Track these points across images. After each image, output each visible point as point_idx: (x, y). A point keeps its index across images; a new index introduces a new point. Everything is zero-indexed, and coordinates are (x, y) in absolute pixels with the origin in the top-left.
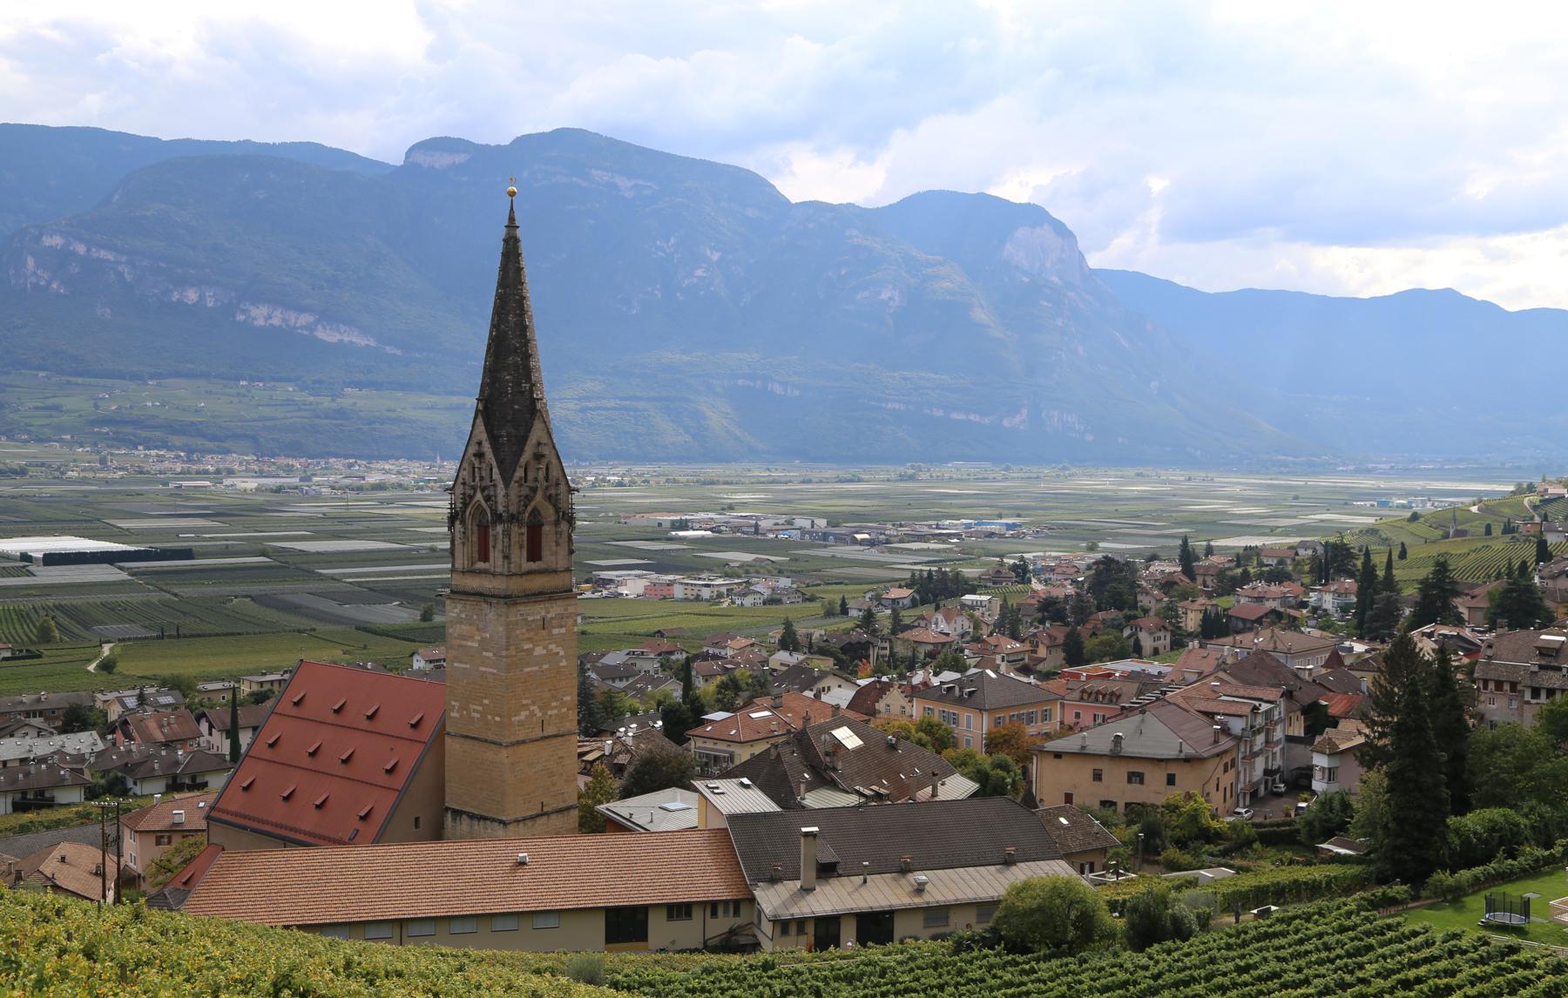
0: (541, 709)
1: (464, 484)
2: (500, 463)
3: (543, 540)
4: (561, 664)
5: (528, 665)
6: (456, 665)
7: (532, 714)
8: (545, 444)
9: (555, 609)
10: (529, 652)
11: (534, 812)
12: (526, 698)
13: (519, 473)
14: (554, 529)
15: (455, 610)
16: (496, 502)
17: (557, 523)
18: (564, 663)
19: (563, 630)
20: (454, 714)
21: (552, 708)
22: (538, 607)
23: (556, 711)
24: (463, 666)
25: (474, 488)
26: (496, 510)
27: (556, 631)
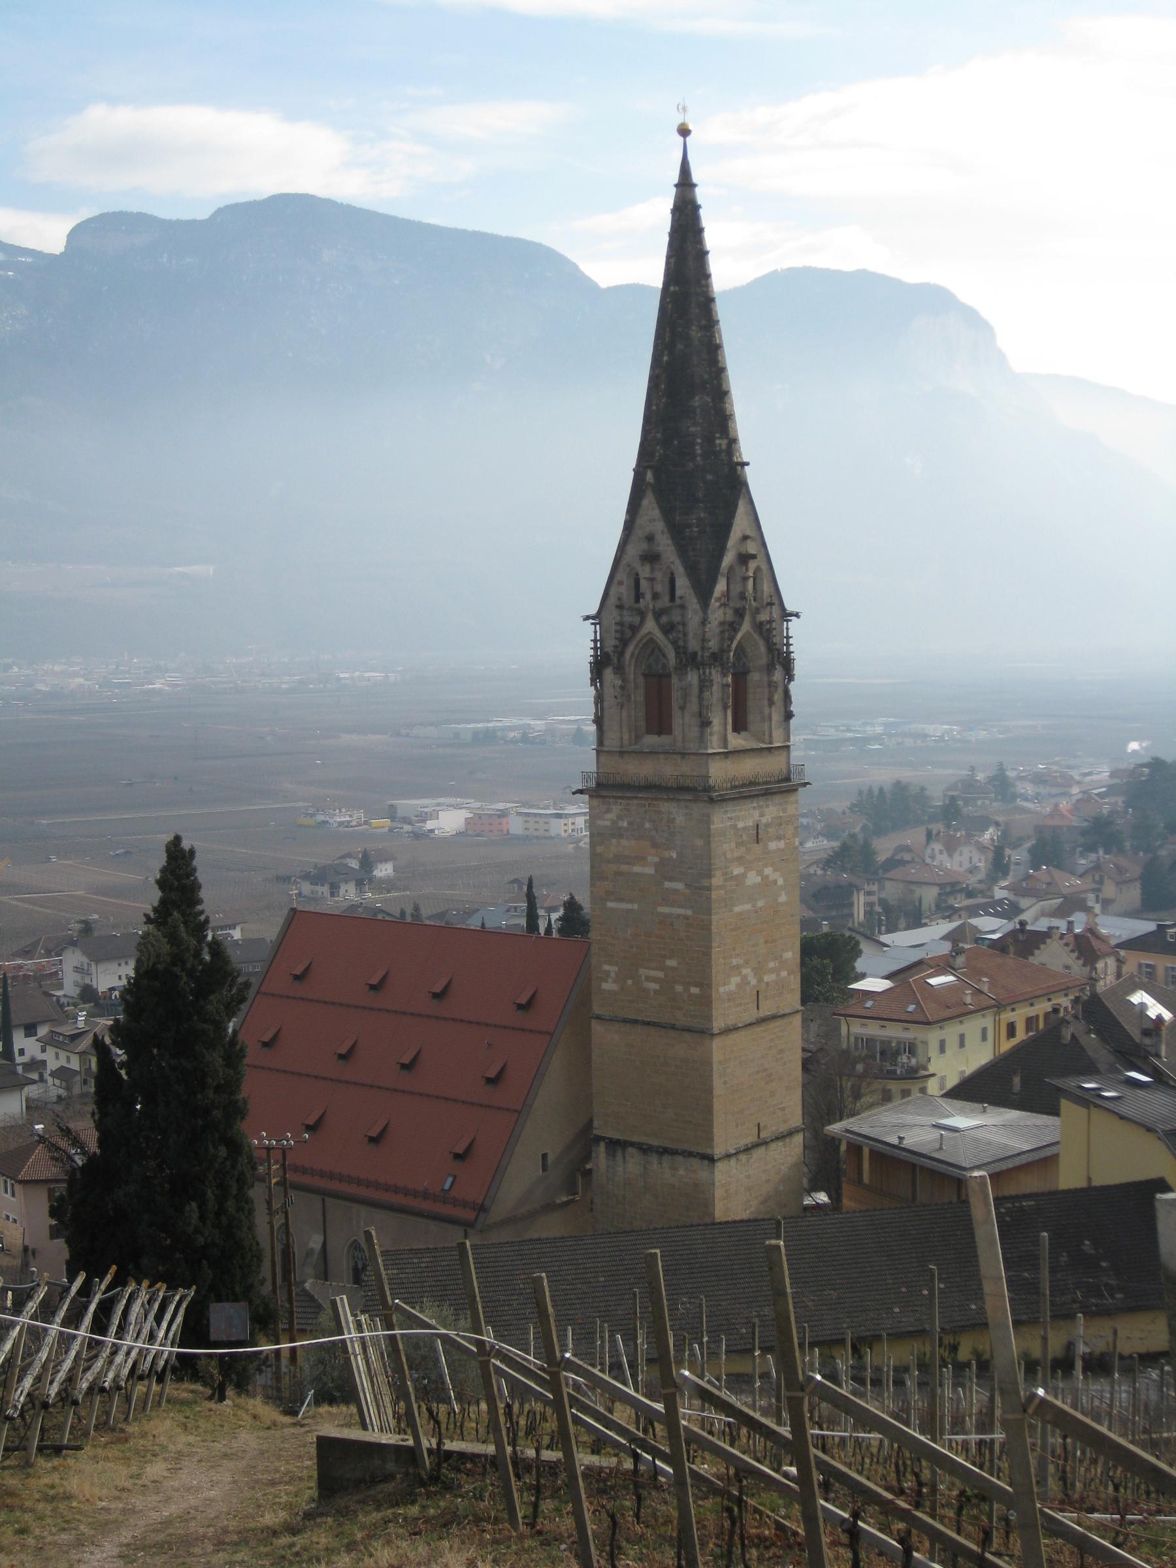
1: (620, 607)
2: (691, 570)
3: (750, 697)
6: (610, 905)
7: (745, 981)
9: (768, 812)
10: (739, 879)
11: (743, 1142)
12: (737, 955)
13: (721, 587)
14: (765, 678)
15: (609, 816)
16: (685, 635)
17: (770, 668)
18: (783, 898)
19: (782, 844)
20: (609, 986)
23: (773, 977)
24: (629, 906)
25: (642, 614)
26: (685, 647)
27: (773, 845)
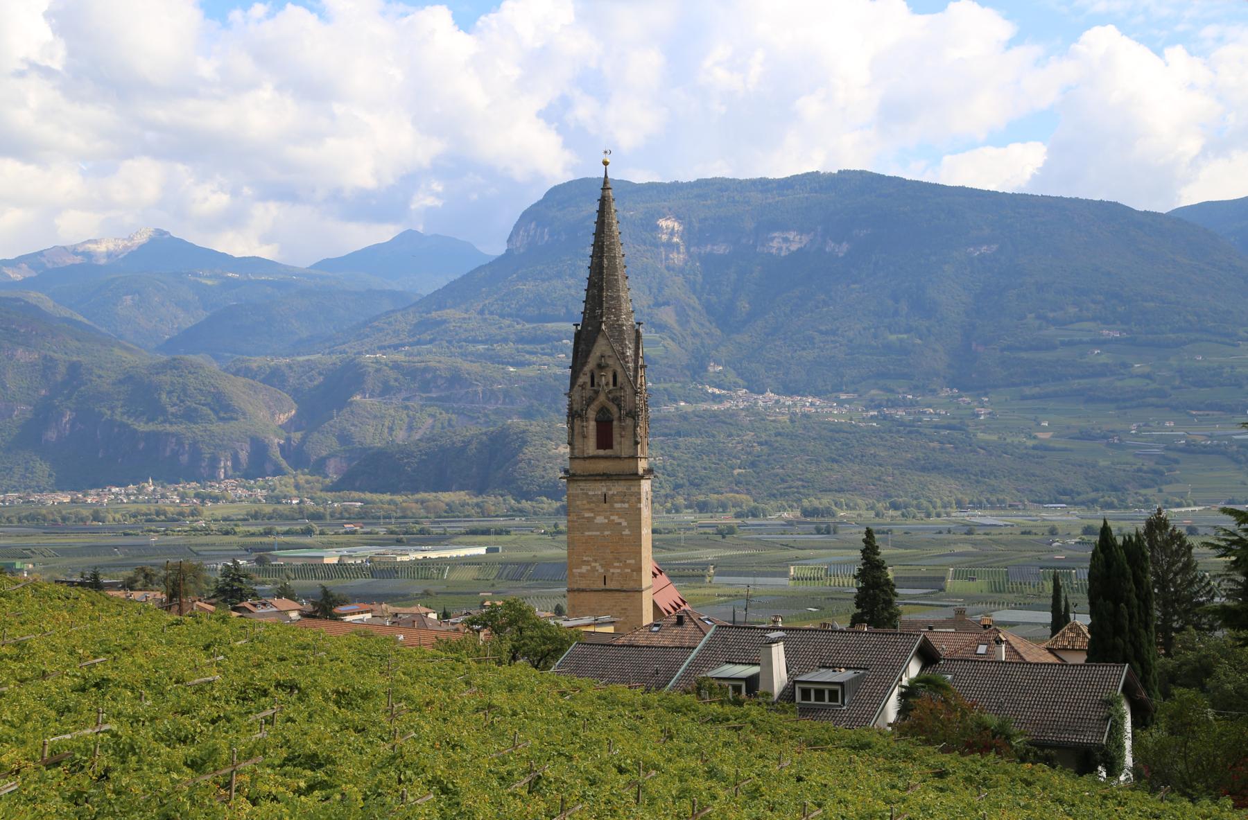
0: (602, 566)
4: (624, 533)
5: (589, 529)
7: (594, 569)
8: (609, 356)
9: (616, 488)
10: (590, 520)
12: (587, 556)
18: (627, 532)
19: (626, 505)
21: (615, 567)
22: (598, 485)
23: (619, 571)
27: (618, 505)
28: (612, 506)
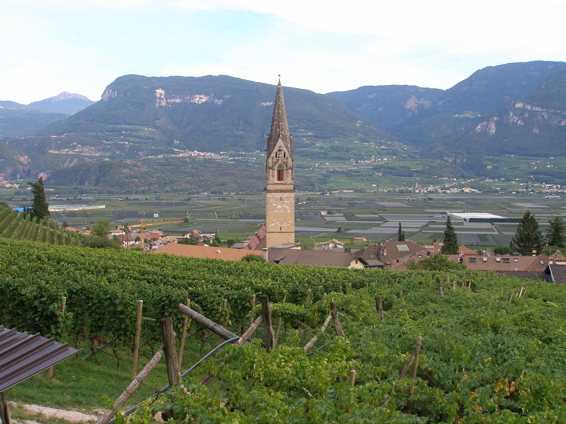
5: (275, 210)
7: (277, 225)
10: (276, 207)
18: (289, 211)
19: (289, 201)
22: (278, 194)
27: (286, 201)
28: (284, 202)
